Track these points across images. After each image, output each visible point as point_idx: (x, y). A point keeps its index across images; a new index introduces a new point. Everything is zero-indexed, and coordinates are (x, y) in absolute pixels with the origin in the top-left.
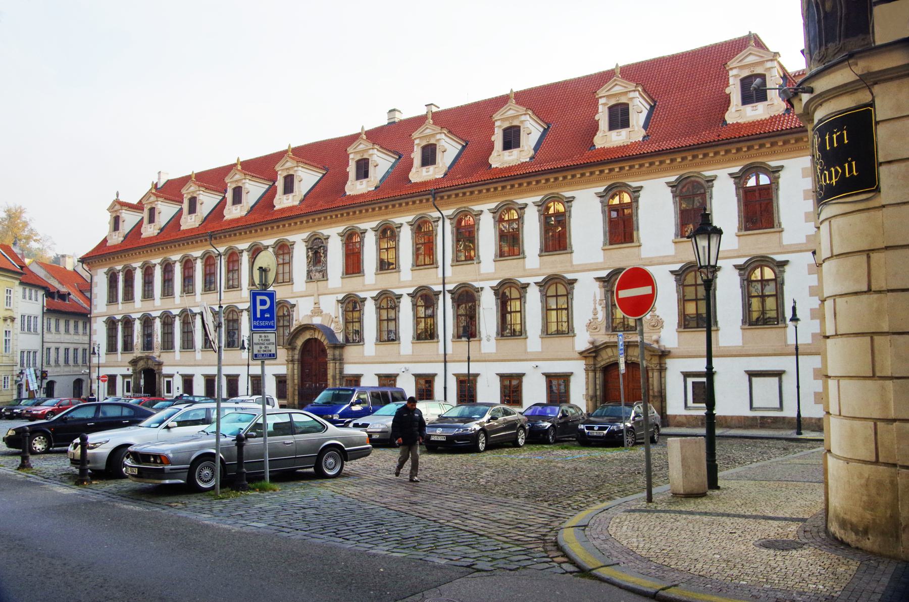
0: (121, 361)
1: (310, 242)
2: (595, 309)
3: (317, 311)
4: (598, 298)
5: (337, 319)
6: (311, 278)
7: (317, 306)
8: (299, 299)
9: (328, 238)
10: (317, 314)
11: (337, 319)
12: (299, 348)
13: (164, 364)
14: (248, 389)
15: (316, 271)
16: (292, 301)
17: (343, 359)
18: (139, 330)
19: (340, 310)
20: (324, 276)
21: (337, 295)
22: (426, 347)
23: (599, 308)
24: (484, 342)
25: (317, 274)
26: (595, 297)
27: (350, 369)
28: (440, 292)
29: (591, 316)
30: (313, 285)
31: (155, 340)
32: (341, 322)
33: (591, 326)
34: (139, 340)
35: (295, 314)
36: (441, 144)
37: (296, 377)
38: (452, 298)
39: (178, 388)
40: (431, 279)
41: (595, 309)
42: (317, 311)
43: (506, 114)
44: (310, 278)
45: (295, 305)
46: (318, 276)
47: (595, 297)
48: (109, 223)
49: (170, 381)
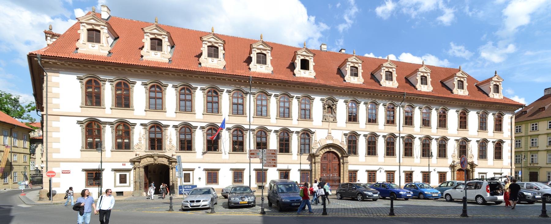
1: (325, 101)
2: (454, 150)
3: (329, 136)
4: (455, 146)
5: (343, 143)
6: (325, 120)
11: (343, 143)
16: (313, 130)
20: (335, 120)
21: (342, 131)
22: (390, 159)
23: (456, 150)
24: (415, 158)
25: (330, 118)
26: (454, 146)
27: (351, 168)
28: (398, 136)
29: (453, 152)
30: (326, 125)
32: (345, 144)
33: (453, 156)
35: (313, 137)
38: (403, 140)
40: (394, 129)
41: (454, 150)
42: (329, 136)
44: (325, 120)
45: (314, 132)
46: (331, 119)
47: (454, 146)
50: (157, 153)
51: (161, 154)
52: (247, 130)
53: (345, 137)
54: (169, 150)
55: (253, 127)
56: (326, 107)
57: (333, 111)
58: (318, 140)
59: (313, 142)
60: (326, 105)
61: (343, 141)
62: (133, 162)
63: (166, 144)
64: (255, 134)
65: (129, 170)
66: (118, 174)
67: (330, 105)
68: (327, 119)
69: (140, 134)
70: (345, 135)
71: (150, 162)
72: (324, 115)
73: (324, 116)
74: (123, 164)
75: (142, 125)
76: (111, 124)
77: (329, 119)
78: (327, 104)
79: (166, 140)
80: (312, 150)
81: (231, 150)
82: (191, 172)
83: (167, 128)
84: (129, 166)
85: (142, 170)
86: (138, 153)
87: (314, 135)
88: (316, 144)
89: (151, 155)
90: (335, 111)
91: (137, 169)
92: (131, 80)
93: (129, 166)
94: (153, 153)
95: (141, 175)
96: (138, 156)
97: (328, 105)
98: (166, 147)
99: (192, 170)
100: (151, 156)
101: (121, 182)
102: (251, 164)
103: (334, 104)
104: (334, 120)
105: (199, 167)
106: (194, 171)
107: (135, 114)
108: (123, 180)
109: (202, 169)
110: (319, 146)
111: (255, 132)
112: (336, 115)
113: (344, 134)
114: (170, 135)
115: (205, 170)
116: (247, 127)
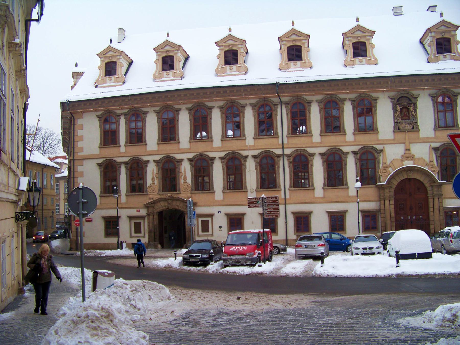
0: (126, 203)
1: (396, 100)
3: (408, 155)
5: (431, 163)
6: (399, 129)
7: (407, 152)
8: (385, 146)
9: (417, 97)
10: (408, 159)
11: (431, 163)
12: (394, 187)
13: (198, 204)
14: (359, 223)
15: (406, 123)
16: (379, 147)
17: (442, 195)
18: (155, 172)
19: (434, 156)
20: (415, 128)
21: (428, 145)
25: (407, 125)
30: (400, 136)
31: (182, 181)
34: (156, 182)
35: (381, 158)
36: (178, 56)
37: (393, 211)
39: (220, 227)
42: (408, 155)
43: (439, 28)
44: (397, 128)
45: (382, 150)
46: (408, 127)
48: (218, 57)
49: (208, 221)
50: (170, 195)
51: (175, 196)
52: (279, 156)
53: (435, 153)
54: (184, 190)
55: (287, 151)
56: (398, 108)
57: (411, 114)
58: (388, 162)
59: (381, 165)
60: (398, 106)
61: (431, 160)
62: (147, 206)
63: (180, 183)
64: (291, 160)
65: (143, 217)
66: (133, 222)
67: (405, 105)
68: (401, 128)
69: (153, 172)
70: (436, 149)
71: (163, 206)
72: (396, 121)
73: (396, 124)
74: (137, 210)
75: (155, 161)
76: (125, 163)
77: (405, 127)
78: (398, 104)
79: (180, 178)
80: (379, 178)
81: (259, 187)
82: (210, 219)
83: (180, 163)
84: (143, 212)
85: (156, 217)
86: (151, 196)
87: (381, 154)
88: (385, 169)
89: (165, 198)
90: (413, 113)
91: (151, 217)
92: (145, 109)
93: (143, 212)
94: (166, 195)
95: (155, 223)
96: (151, 200)
97: (402, 105)
98: (181, 188)
99: (211, 216)
100: (165, 200)
101: (136, 232)
102: (287, 205)
103: (411, 102)
104: (413, 128)
105: (219, 212)
106: (214, 218)
107: (148, 150)
108: (138, 229)
109: (223, 213)
110: (392, 171)
111: (291, 159)
112: (417, 120)
113: (433, 149)
114: (185, 171)
115: (227, 215)
116: (279, 152)
